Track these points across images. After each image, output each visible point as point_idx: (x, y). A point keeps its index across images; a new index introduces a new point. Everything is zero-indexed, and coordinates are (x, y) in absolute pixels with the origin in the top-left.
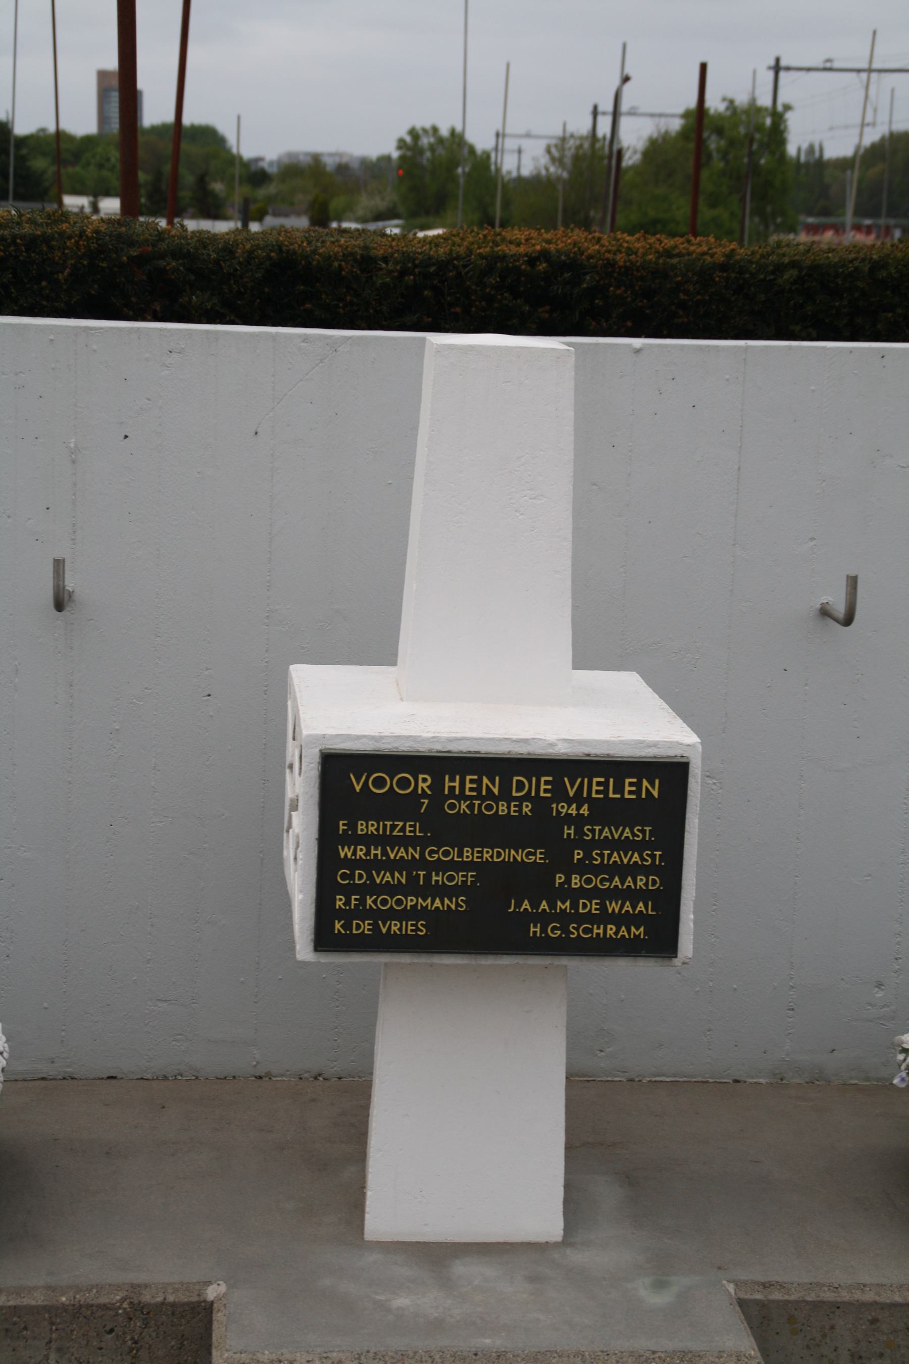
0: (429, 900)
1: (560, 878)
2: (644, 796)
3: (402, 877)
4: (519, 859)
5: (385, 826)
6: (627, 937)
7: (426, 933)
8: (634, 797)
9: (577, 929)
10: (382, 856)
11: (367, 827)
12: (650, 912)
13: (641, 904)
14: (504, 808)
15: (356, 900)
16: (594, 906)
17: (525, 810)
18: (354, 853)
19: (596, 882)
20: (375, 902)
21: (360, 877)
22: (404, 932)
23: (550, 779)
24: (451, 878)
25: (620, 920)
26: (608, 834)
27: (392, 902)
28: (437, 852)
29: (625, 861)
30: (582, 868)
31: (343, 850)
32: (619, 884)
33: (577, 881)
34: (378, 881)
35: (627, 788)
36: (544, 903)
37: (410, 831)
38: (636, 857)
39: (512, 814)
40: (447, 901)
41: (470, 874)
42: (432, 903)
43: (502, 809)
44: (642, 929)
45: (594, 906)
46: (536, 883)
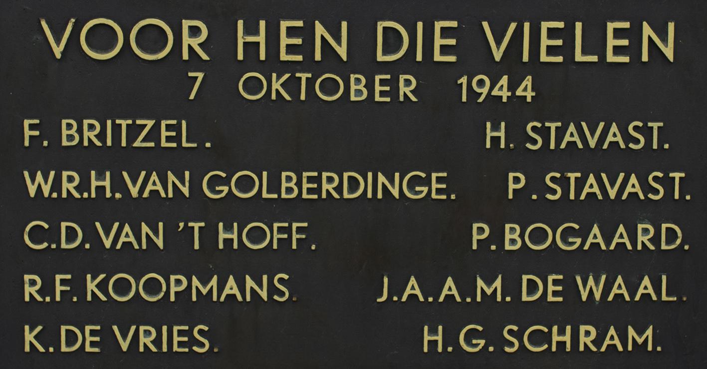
0: (214, 282)
1: (480, 232)
2: (645, 58)
3: (156, 233)
4: (395, 193)
5: (117, 128)
6: (620, 348)
7: (211, 348)
8: (626, 59)
9: (519, 335)
10: (113, 192)
11: (80, 131)
12: (664, 298)
13: (646, 281)
14: (361, 87)
15: (63, 282)
16: (551, 288)
17: (403, 89)
18: (57, 186)
19: (554, 237)
20: (103, 286)
21: (70, 237)
22: (165, 349)
23: (454, 24)
24: (257, 235)
25: (605, 314)
26: (576, 139)
27: (137, 287)
28: (226, 182)
29: (612, 193)
30: (525, 209)
31: (33, 180)
32: (600, 240)
33: (516, 236)
34: (108, 244)
35: (611, 42)
36: (450, 282)
37: (168, 139)
38: (634, 185)
39: (378, 98)
40: (250, 283)
41: (295, 225)
42: (221, 289)
43: (358, 89)
44: (649, 332)
45: (551, 288)
46: (436, 242)
